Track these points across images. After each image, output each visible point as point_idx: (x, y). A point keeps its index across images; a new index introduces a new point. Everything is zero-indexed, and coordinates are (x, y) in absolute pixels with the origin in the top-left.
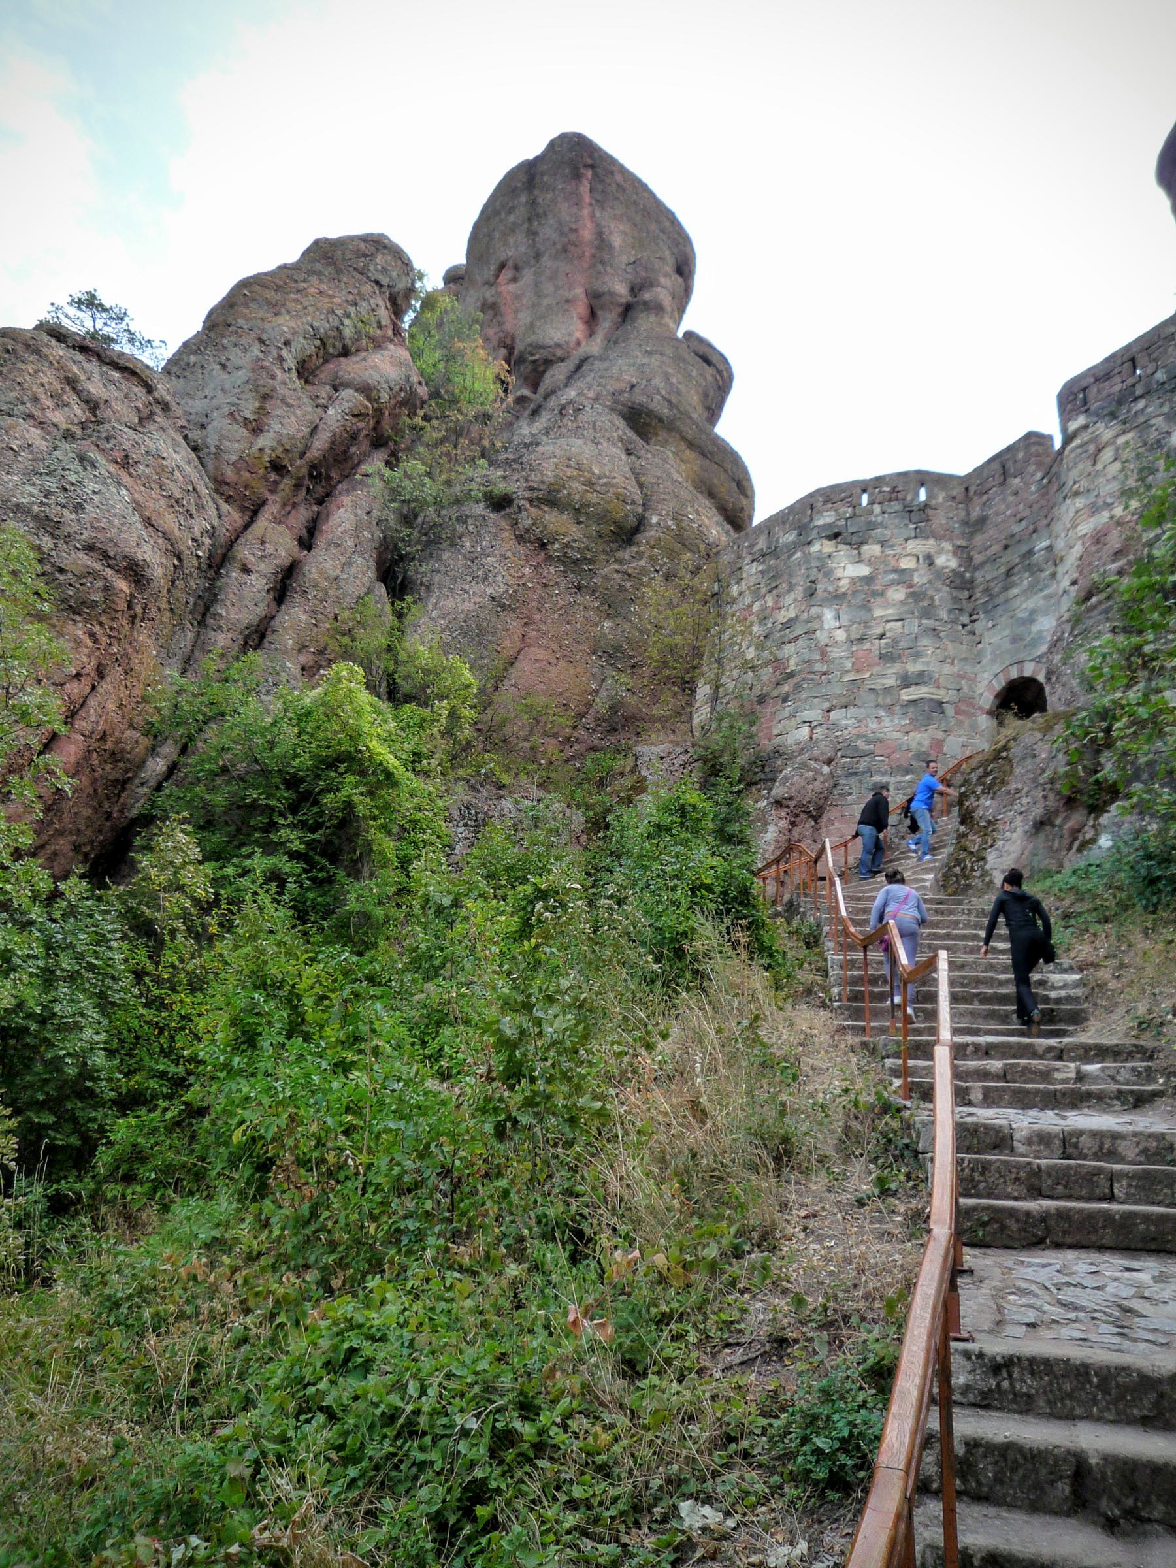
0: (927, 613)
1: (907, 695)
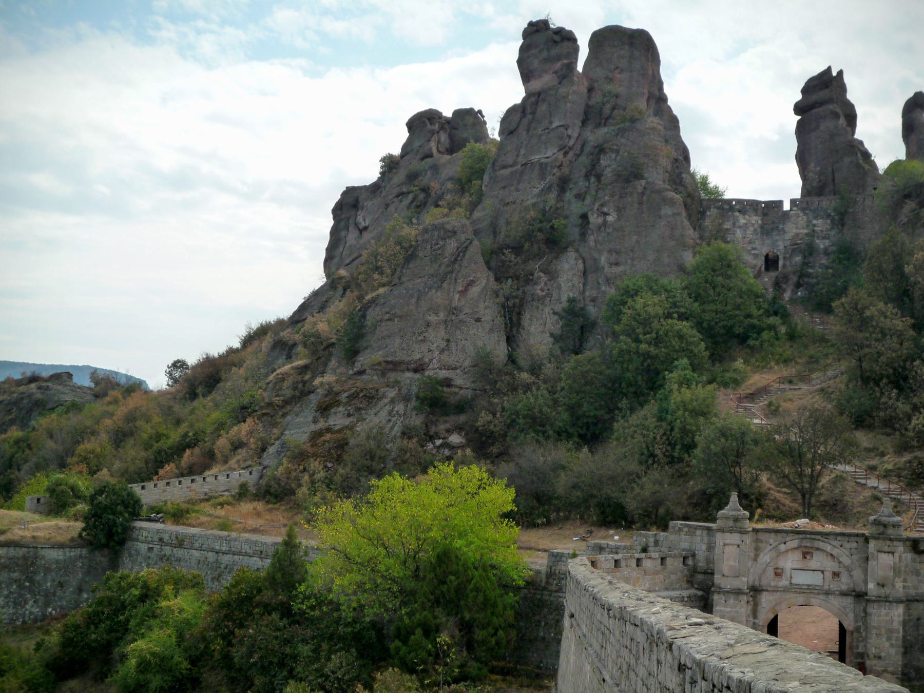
0: (757, 234)
1: (753, 252)
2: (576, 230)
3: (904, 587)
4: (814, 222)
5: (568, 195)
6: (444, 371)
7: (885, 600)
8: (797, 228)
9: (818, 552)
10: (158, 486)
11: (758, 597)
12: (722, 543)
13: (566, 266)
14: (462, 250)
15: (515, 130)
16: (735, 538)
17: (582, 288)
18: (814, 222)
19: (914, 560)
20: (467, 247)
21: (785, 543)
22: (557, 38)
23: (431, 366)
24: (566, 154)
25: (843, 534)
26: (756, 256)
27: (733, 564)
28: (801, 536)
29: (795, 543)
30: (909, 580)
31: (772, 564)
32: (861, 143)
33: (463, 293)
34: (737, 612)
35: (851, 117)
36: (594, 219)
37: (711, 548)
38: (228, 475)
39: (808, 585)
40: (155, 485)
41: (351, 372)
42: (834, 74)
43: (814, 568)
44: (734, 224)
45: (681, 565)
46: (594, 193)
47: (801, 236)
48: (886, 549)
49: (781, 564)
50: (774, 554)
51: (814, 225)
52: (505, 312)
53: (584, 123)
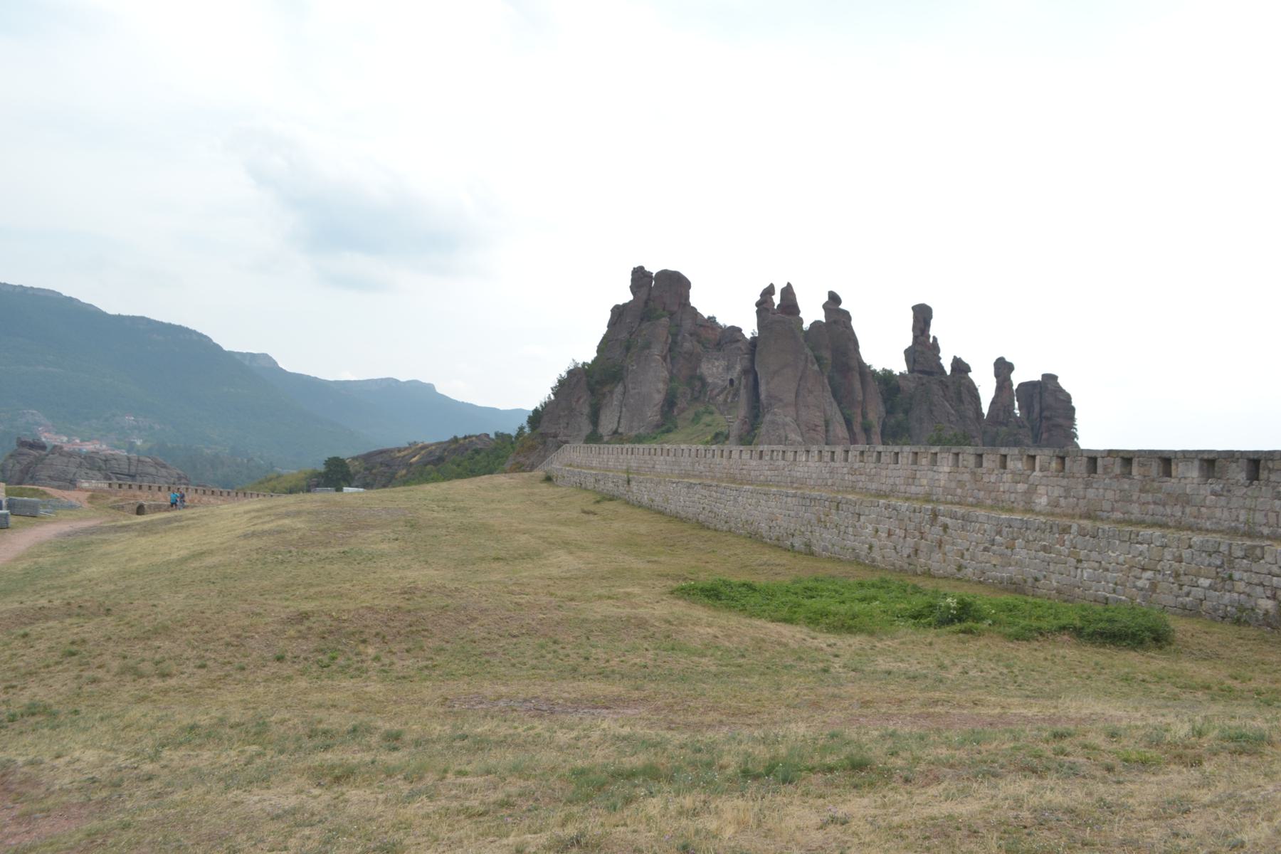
26: (723, 381)
33: (577, 401)
36: (630, 368)
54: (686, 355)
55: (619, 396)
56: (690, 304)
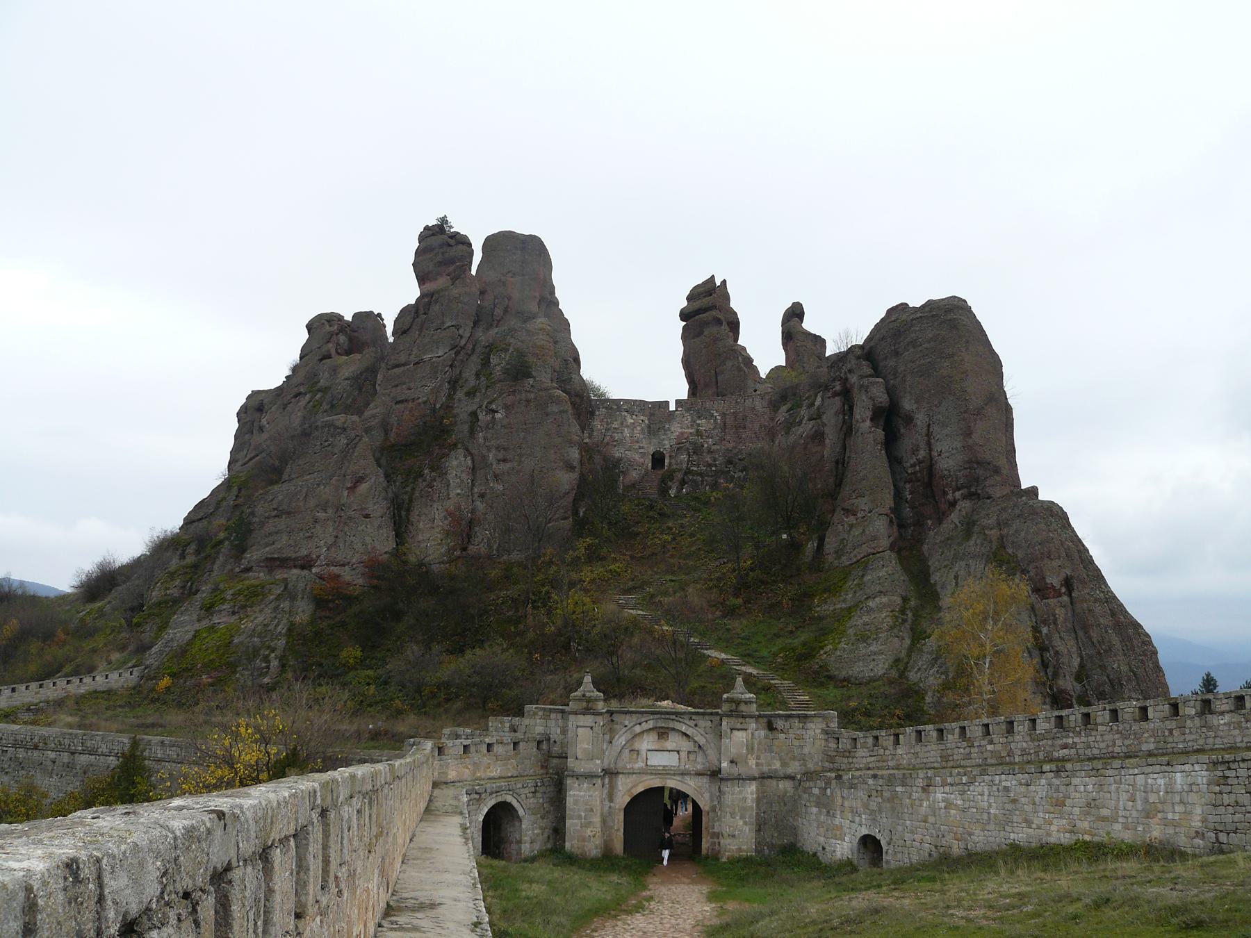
2: (466, 427)
3: (757, 765)
4: (699, 422)
5: (460, 394)
6: (332, 568)
7: (739, 779)
8: (681, 428)
9: (673, 733)
10: (30, 688)
11: (614, 779)
12: (575, 726)
13: (455, 463)
14: (352, 445)
15: (408, 329)
16: (588, 720)
17: (470, 484)
18: (699, 422)
19: (766, 737)
20: (357, 444)
21: (640, 724)
22: (452, 242)
23: (319, 562)
24: (457, 353)
25: (697, 714)
26: (643, 454)
27: (587, 746)
28: (656, 716)
29: (651, 724)
30: (762, 756)
31: (628, 745)
32: (744, 349)
33: (352, 489)
34: (591, 796)
35: (734, 325)
36: (483, 417)
37: (564, 731)
38: (107, 676)
39: (664, 766)
40: (27, 688)
41: (237, 570)
42: (718, 284)
43: (669, 749)
44: (622, 423)
45: (535, 750)
46: (483, 391)
47: (686, 436)
48: (739, 726)
49: (637, 746)
50: (629, 736)
51: (698, 425)
52: (394, 508)
53: (476, 323)
54: (578, 400)
55: (464, 476)
56: (557, 303)
